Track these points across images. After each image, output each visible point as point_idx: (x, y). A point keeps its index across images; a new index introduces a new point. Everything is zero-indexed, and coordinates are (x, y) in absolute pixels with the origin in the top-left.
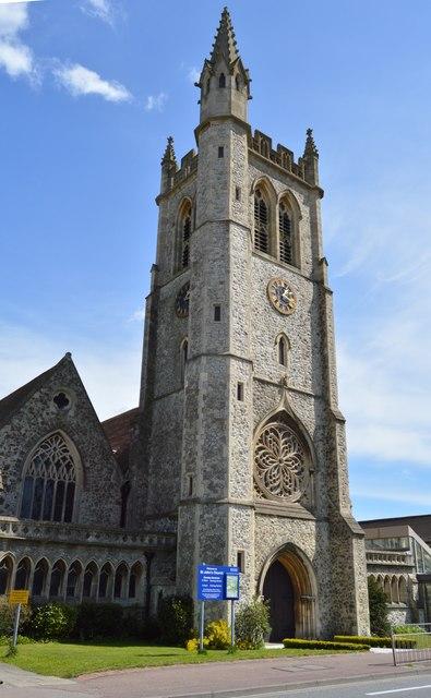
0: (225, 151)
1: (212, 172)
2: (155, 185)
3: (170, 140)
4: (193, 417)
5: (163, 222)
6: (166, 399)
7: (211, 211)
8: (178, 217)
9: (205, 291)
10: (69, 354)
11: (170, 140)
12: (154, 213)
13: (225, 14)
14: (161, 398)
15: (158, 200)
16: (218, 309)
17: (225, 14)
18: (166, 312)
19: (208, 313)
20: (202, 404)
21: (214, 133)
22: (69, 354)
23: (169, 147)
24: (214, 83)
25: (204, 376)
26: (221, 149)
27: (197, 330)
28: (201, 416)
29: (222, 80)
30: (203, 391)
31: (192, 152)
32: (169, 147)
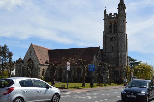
1: (123, 24)
3: (105, 8)
4: (122, 58)
6: (109, 53)
7: (123, 30)
8: (109, 24)
9: (123, 42)
10: (99, 46)
11: (105, 8)
14: (109, 53)
15: (104, 19)
16: (124, 45)
19: (123, 46)
20: (123, 57)
21: (123, 18)
22: (99, 46)
23: (105, 9)
24: (122, 8)
25: (123, 54)
26: (124, 21)
27: (121, 48)
29: (123, 9)
31: (111, 14)
32: (105, 9)
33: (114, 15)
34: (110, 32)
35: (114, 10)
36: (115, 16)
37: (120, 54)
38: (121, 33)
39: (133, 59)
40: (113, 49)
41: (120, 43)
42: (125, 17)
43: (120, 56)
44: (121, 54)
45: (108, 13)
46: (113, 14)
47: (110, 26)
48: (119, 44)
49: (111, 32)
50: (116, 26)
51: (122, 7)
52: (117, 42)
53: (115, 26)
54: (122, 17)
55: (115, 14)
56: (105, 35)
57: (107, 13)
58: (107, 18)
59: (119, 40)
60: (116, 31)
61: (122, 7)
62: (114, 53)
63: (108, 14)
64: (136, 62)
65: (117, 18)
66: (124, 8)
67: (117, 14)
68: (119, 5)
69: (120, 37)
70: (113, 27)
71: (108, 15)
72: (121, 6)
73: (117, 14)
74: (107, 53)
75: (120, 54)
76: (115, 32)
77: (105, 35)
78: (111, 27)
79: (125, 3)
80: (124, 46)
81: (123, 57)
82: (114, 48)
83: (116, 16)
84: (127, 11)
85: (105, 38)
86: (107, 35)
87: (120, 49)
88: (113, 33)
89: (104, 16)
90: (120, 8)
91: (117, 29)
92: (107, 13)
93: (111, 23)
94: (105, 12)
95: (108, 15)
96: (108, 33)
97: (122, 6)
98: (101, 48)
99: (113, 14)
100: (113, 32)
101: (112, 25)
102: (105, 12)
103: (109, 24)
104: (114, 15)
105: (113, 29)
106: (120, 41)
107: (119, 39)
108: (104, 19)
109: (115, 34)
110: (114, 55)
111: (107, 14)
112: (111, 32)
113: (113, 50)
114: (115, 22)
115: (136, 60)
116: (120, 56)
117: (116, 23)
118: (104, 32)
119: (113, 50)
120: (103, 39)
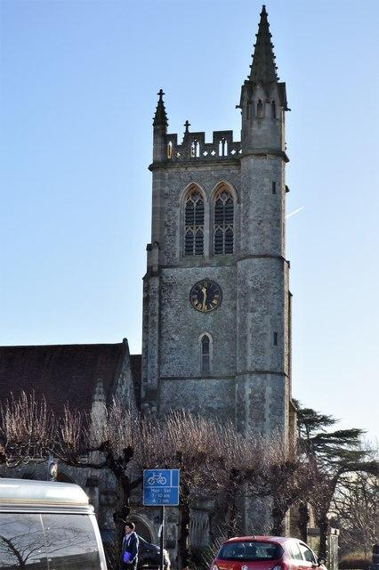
0: (277, 186)
2: (146, 151)
3: (161, 94)
5: (159, 196)
6: (181, 383)
10: (125, 340)
11: (161, 94)
12: (144, 184)
13: (264, 15)
14: (182, 379)
15: (151, 168)
16: (276, 334)
17: (264, 15)
18: (178, 297)
19: (270, 338)
20: (268, 411)
22: (125, 340)
23: (161, 102)
24: (268, 108)
25: (269, 390)
28: (268, 420)
30: (269, 401)
31: (200, 136)
32: (161, 102)
33: (214, 146)
34: (188, 250)
35: (216, 112)
36: (223, 149)
37: (249, 392)
38: (256, 261)
39: (310, 412)
40: (206, 360)
41: (250, 324)
42: (287, 160)
43: (249, 402)
44: (255, 391)
46: (209, 139)
47: (189, 211)
48: (243, 326)
49: (192, 246)
50: (224, 214)
51: (264, 90)
52: (230, 315)
53: (215, 208)
54: (266, 163)
55: (218, 136)
56: (161, 267)
57: (170, 131)
58: (172, 155)
59: (246, 304)
60: (224, 244)
61: (264, 90)
62: (214, 382)
63: (174, 137)
64: (330, 429)
65: (235, 161)
66: (279, 109)
67: (237, 138)
68: (248, 88)
69: (250, 284)
70: (207, 216)
72: (259, 94)
73: (237, 138)
74: (167, 384)
75: (249, 392)
76: (217, 248)
77: (155, 269)
78: (194, 215)
79: (282, 75)
80: (276, 343)
81: (266, 406)
82: (211, 346)
83: (229, 151)
84: (295, 131)
85: (161, 288)
86: (171, 267)
87: (250, 357)
88: (211, 255)
89: (155, 143)
90: (250, 102)
91: (229, 236)
92: (170, 131)
94: (160, 119)
95: (180, 141)
96: (177, 255)
97: (267, 94)
98: (136, 348)
99: (209, 139)
100: (206, 252)
101: (200, 203)
102: (160, 119)
103: (182, 195)
104: (214, 146)
105: (206, 232)
106: (253, 311)
107: (245, 296)
108: (151, 168)
109: (221, 264)
110: (212, 397)
111: (174, 137)
112: (192, 246)
115: (326, 420)
116: (249, 402)
117: (226, 192)
118: (149, 248)
119: (205, 369)
120: (146, 289)
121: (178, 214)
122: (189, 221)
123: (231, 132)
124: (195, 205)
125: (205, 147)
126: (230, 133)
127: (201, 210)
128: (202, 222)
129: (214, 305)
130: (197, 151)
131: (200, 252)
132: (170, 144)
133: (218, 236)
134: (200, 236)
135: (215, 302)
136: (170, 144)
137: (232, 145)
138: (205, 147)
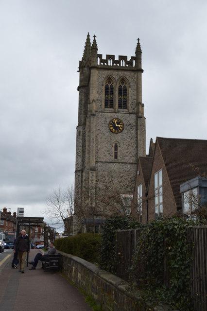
33: (119, 62)
34: (106, 106)
45: (103, 51)
46: (117, 58)
47: (106, 88)
49: (109, 103)
50: (123, 92)
56: (96, 112)
57: (99, 53)
60: (123, 105)
70: (116, 93)
71: (104, 58)
74: (99, 164)
76: (120, 107)
78: (109, 91)
92: (99, 53)
93: (109, 79)
95: (104, 58)
99: (117, 58)
104: (119, 62)
111: (100, 56)
113: (116, 157)
114: (123, 80)
119: (116, 157)
121: (95, 92)
122: (106, 93)
123: (127, 57)
124: (109, 86)
125: (114, 62)
126: (127, 57)
127: (112, 88)
128: (112, 93)
129: (120, 130)
130: (110, 63)
131: (112, 106)
132: (99, 59)
133: (120, 101)
134: (112, 101)
135: (121, 128)
136: (99, 59)
137: (127, 62)
138: (114, 62)
